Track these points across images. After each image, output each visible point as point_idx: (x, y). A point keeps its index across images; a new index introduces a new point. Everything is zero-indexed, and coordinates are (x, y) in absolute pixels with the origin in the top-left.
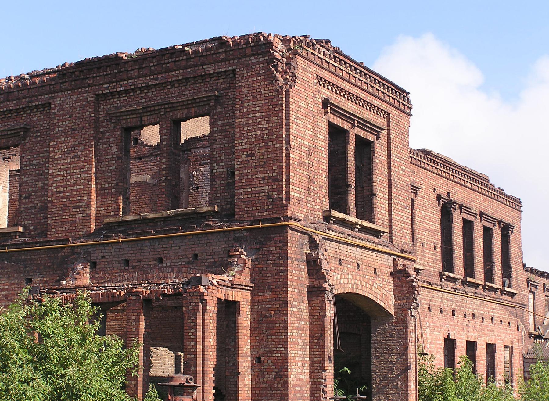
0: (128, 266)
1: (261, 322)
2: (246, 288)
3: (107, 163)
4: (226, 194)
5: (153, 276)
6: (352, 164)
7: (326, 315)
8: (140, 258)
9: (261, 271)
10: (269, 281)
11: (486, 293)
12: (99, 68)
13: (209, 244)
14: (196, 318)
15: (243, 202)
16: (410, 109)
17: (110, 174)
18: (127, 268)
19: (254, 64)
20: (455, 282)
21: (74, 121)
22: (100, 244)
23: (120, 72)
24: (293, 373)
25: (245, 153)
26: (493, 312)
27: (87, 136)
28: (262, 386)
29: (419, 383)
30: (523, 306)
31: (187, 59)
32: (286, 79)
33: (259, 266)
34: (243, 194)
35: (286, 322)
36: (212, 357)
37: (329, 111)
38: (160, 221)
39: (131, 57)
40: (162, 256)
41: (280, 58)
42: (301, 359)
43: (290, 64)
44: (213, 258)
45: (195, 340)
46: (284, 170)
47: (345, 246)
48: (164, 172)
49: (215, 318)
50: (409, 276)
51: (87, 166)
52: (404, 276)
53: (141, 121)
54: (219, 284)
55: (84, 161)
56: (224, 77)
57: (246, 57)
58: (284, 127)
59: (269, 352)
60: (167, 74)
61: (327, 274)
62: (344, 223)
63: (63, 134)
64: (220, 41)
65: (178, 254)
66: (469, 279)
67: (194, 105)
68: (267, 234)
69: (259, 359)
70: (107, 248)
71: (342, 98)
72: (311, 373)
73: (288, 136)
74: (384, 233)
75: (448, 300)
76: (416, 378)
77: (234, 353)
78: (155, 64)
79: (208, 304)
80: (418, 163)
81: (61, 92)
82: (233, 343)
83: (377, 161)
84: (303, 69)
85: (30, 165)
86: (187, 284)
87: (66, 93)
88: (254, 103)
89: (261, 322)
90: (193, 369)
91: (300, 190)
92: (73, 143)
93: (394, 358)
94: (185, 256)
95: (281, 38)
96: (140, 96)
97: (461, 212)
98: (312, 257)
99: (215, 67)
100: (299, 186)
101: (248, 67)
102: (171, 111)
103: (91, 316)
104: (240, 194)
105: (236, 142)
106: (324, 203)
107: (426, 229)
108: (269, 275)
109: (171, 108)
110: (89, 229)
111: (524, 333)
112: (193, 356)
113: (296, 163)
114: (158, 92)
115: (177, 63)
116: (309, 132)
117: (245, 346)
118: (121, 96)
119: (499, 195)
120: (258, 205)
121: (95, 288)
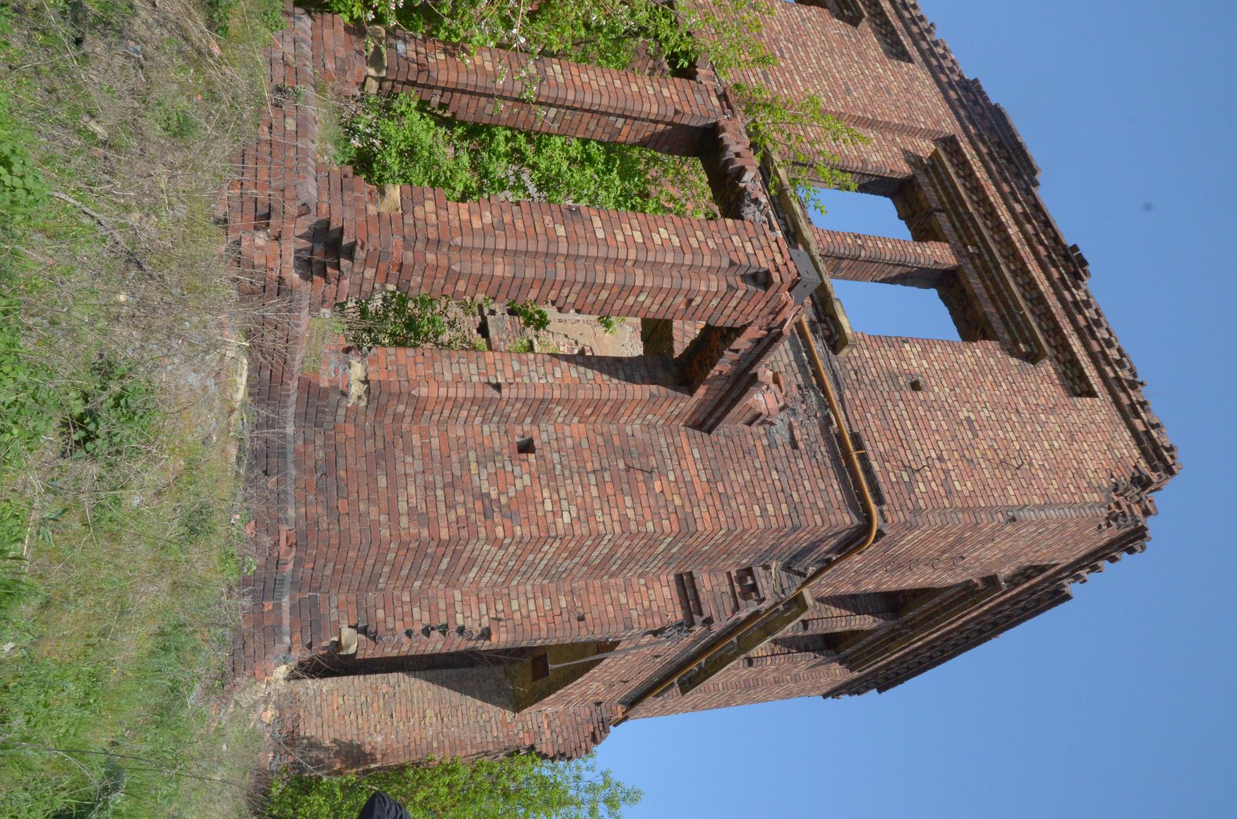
28: (455, 457)
33: (760, 449)
85: (803, 20)
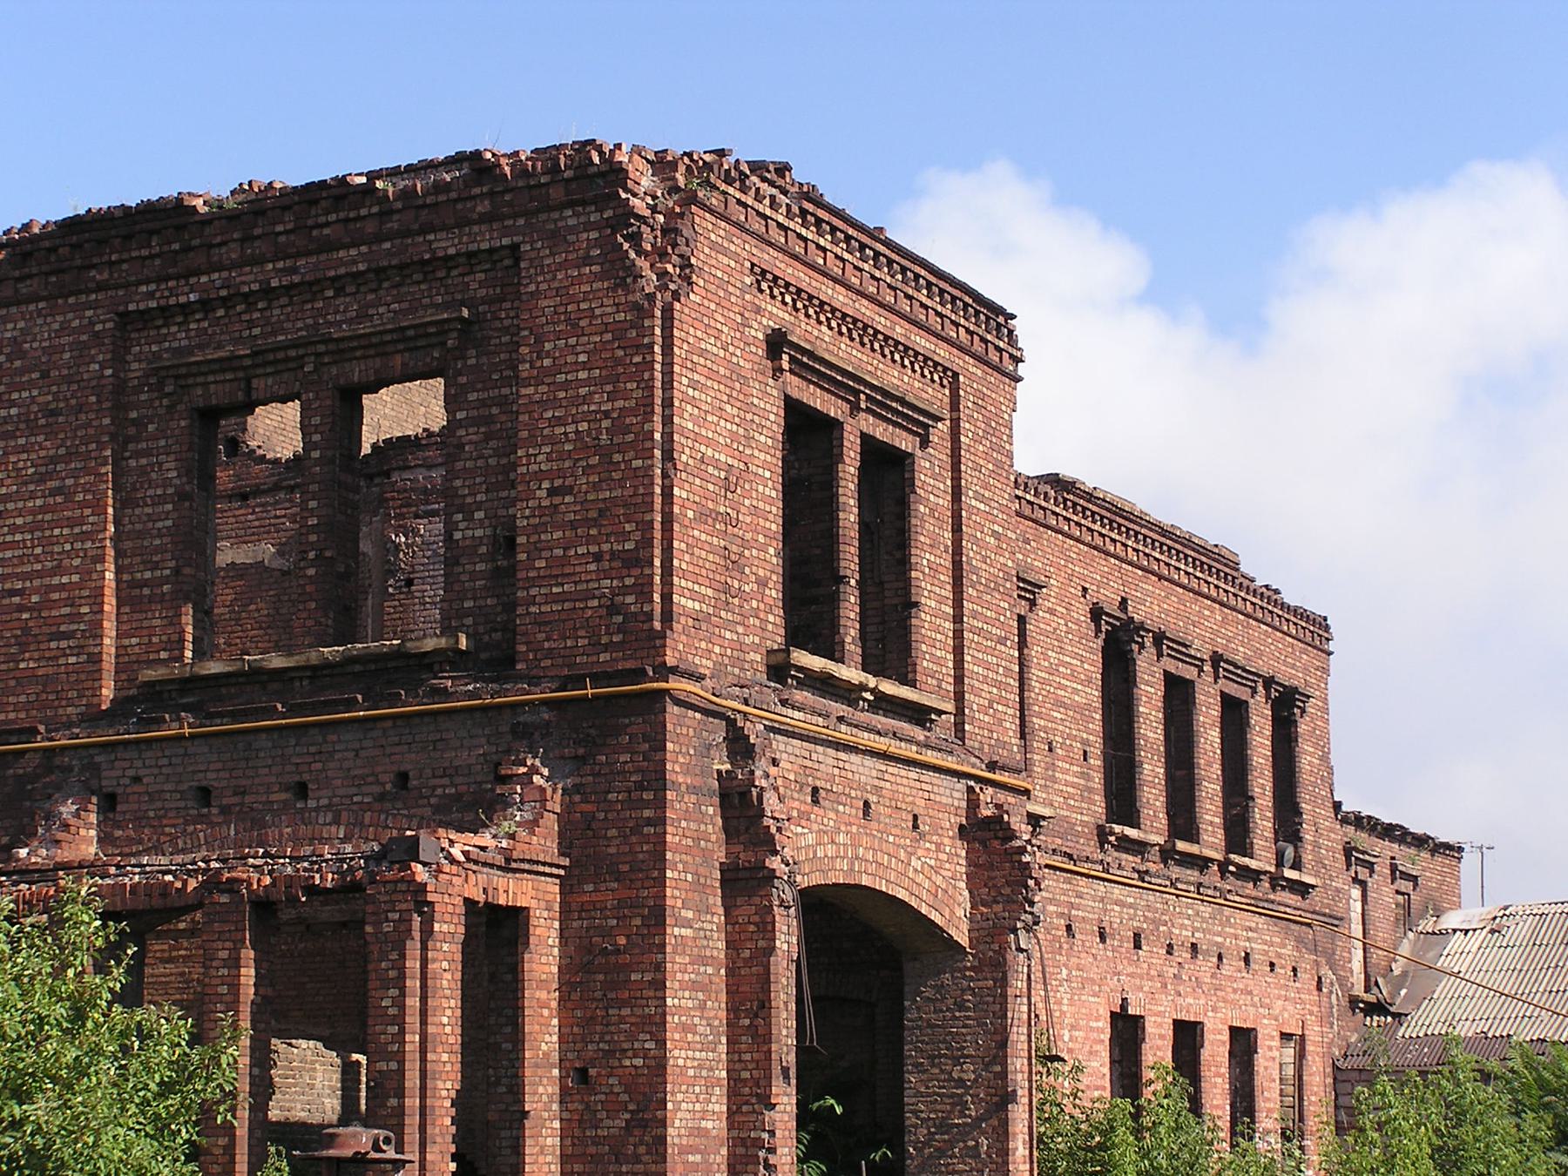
0: (208, 805)
1: (587, 968)
2: (547, 870)
3: (149, 510)
4: (489, 601)
5: (281, 835)
6: (849, 516)
7: (774, 948)
8: (244, 782)
9: (589, 819)
10: (612, 850)
11: (1230, 883)
12: (128, 238)
13: (440, 745)
14: (403, 957)
15: (540, 624)
16: (1017, 360)
17: (158, 542)
18: (205, 810)
19: (573, 230)
20: (1142, 854)
21: (54, 389)
22: (128, 742)
23: (187, 249)
24: (679, 1115)
25: (546, 485)
26: (1248, 939)
27: (91, 431)
28: (592, 1150)
29: (1038, 1142)
30: (1335, 921)
31: (381, 214)
32: (662, 274)
34: (538, 600)
35: (660, 967)
36: (448, 1067)
37: (786, 366)
38: (301, 679)
39: (220, 207)
40: (306, 777)
41: (647, 213)
42: (704, 1073)
43: (677, 231)
44: (452, 785)
45: (399, 1020)
46: (658, 534)
47: (831, 751)
48: (313, 538)
49: (458, 957)
50: (1011, 835)
51: (91, 519)
52: (997, 838)
53: (249, 390)
54: (468, 860)
55: (83, 505)
56: (488, 266)
57: (551, 209)
58: (658, 409)
59: (610, 1053)
60: (323, 257)
61: (779, 829)
62: (825, 685)
63: (22, 426)
64: (474, 165)
65: (353, 773)
66: (1181, 846)
67: (401, 346)
68: (608, 719)
69: (582, 1075)
70: (149, 754)
71: (824, 328)
72: (731, 1114)
73: (668, 437)
74: (940, 713)
75: (1123, 905)
76: (1030, 1128)
77: (512, 1056)
78: (290, 226)
79: (437, 916)
80: (1039, 514)
81: (18, 303)
82: (509, 1029)
83: (922, 508)
84: (714, 246)
86: (377, 858)
87: (32, 307)
88: (572, 341)
89: (587, 968)
90: (393, 1102)
91: (703, 590)
92: (52, 452)
93: (968, 1072)
94: (370, 779)
95: (651, 157)
96: (246, 317)
97: (1160, 655)
98: (735, 783)
99: (460, 237)
100: (700, 580)
101: (556, 238)
102: (335, 362)
103: (99, 950)
104: (532, 601)
105: (520, 453)
106: (770, 627)
107: (1059, 704)
108: (613, 832)
109: (332, 352)
110: (95, 700)
111: (1337, 998)
112: (394, 1066)
113: (690, 514)
114: (296, 308)
115: (351, 226)
116: (729, 426)
117: (543, 1036)
118: (190, 318)
119: (1268, 606)
120: (582, 633)
121: (113, 870)
